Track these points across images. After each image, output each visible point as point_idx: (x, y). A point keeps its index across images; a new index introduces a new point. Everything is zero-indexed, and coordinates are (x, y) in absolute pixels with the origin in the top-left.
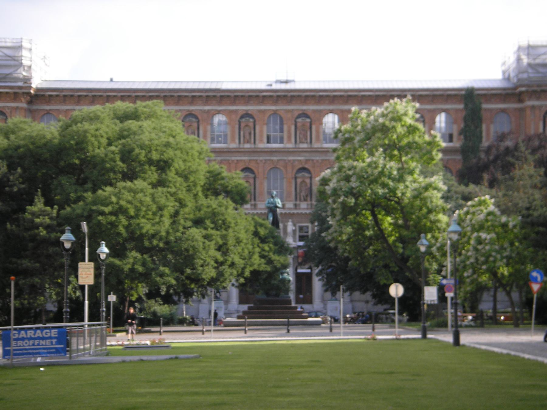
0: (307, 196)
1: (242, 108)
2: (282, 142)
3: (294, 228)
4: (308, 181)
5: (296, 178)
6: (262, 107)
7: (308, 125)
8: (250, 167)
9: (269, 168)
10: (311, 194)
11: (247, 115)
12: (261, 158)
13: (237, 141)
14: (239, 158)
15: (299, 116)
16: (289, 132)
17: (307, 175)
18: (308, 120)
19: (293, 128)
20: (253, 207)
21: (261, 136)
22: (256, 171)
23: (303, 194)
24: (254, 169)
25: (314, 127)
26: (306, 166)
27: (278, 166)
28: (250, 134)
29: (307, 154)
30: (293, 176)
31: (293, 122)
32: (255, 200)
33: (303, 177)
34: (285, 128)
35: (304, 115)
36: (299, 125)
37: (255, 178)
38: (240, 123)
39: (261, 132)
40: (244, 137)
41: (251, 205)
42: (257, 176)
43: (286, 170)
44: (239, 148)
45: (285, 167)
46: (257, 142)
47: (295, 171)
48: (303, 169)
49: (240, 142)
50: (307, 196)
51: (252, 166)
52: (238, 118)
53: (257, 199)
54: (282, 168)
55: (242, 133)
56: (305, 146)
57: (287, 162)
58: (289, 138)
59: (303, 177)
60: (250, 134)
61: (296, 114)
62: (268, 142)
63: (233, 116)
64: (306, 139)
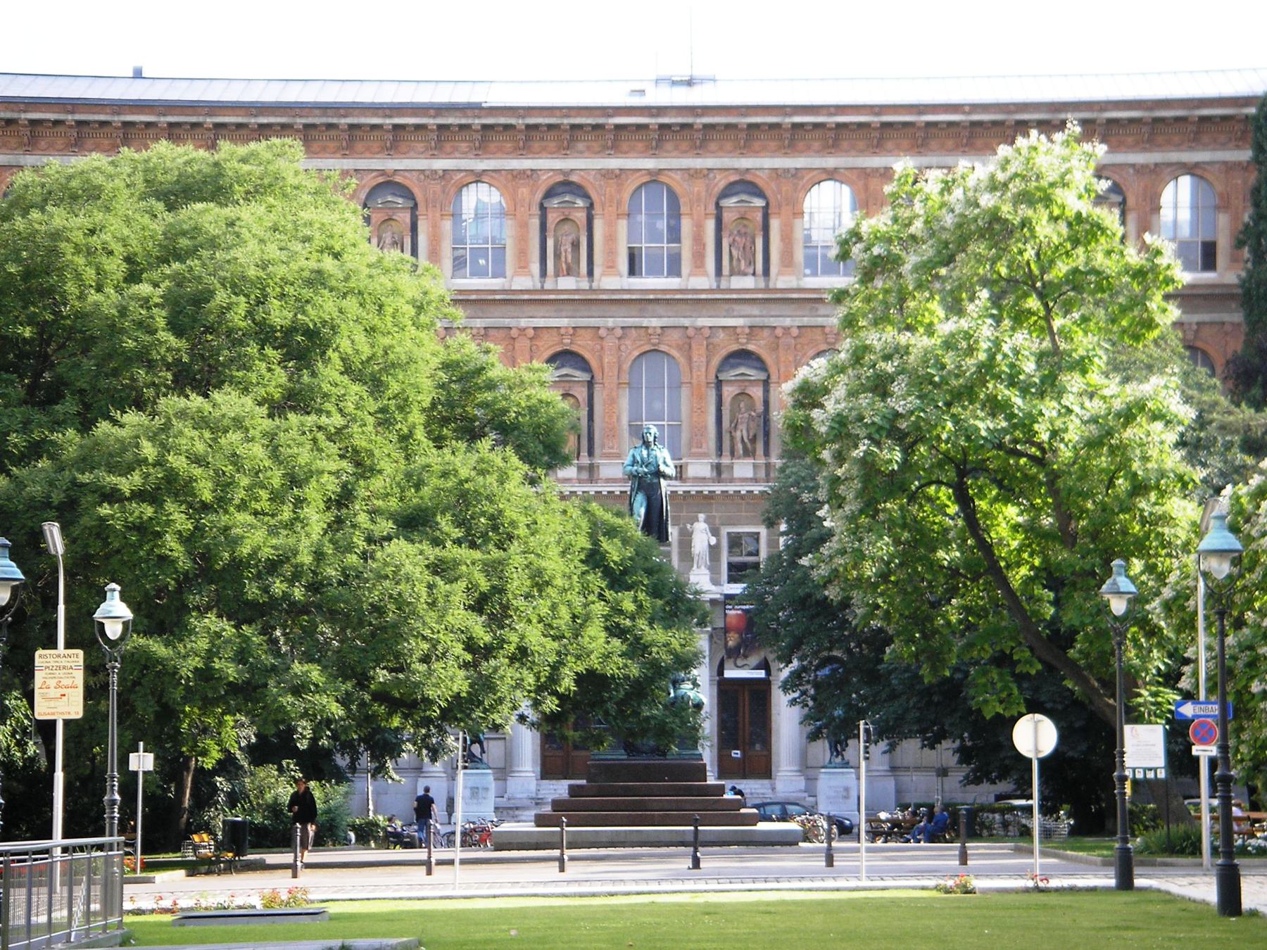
0: (753, 440)
1: (549, 164)
2: (675, 270)
3: (713, 541)
4: (757, 392)
5: (719, 384)
6: (614, 163)
7: (759, 216)
8: (574, 348)
9: (636, 353)
10: (767, 434)
11: (566, 186)
12: (610, 322)
13: (535, 267)
14: (541, 322)
15: (727, 192)
16: (698, 240)
17: (754, 374)
18: (759, 203)
19: (710, 225)
20: (585, 475)
21: (611, 253)
22: (594, 364)
24: (587, 356)
25: (775, 224)
26: (751, 347)
27: (663, 348)
28: (576, 245)
29: (755, 310)
30: (712, 378)
31: (712, 209)
32: (591, 453)
33: (743, 381)
34: (686, 225)
35: (745, 185)
36: (728, 217)
37: (590, 384)
38: (543, 208)
39: (611, 239)
40: (557, 256)
41: (580, 468)
42: (598, 377)
43: (690, 359)
44: (543, 291)
45: (687, 348)
46: (597, 271)
47: (716, 361)
48: (743, 356)
49: (544, 273)
50: (753, 440)
51: (583, 346)
52: (539, 195)
53: (597, 451)
54: (674, 352)
55: (550, 243)
56: (748, 282)
57: (691, 332)
58: (699, 257)
59: (743, 381)
60: (576, 245)
61: (721, 182)
62: (633, 271)
63: (524, 191)
64: (752, 262)
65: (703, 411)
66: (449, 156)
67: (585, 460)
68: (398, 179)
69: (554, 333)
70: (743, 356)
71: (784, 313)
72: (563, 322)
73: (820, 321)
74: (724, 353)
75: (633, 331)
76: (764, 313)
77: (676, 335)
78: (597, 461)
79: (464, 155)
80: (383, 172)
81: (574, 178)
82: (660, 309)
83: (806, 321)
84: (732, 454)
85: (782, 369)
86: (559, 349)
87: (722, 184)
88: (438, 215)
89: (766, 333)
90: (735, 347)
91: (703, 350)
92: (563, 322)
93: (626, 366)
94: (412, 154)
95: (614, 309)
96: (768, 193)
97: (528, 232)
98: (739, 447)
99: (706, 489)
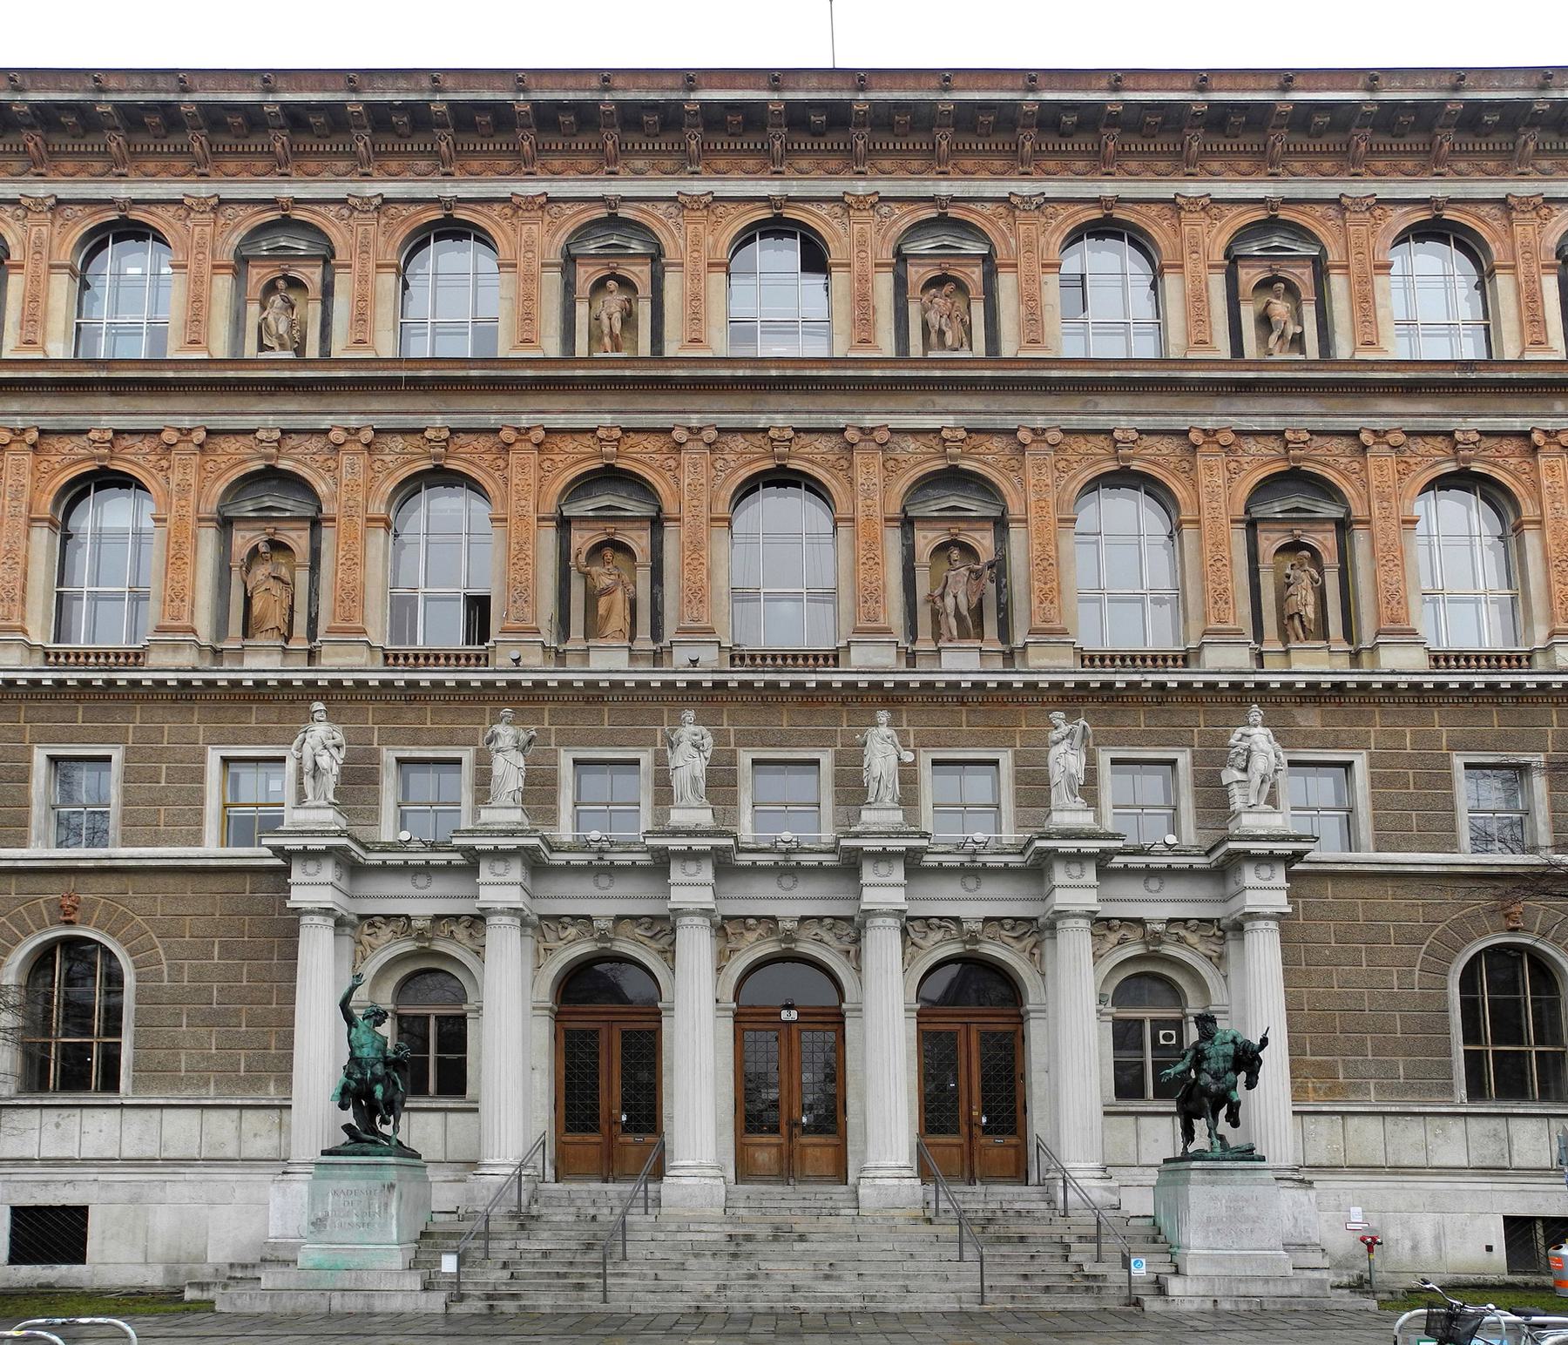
0: (978, 612)
7: (974, 275)
9: (745, 473)
10: (1005, 612)
12: (695, 420)
14: (560, 421)
17: (975, 506)
18: (974, 248)
23: (959, 595)
24: (650, 476)
25: (1006, 283)
28: (629, 318)
29: (975, 403)
33: (955, 517)
41: (633, 657)
50: (978, 612)
51: (641, 458)
52: (561, 239)
55: (582, 310)
59: (955, 517)
60: (629, 318)
61: (905, 218)
65: (875, 561)
66: (393, 176)
67: (644, 642)
68: (299, 214)
69: (587, 440)
70: (954, 478)
71: (1035, 409)
72: (607, 419)
73: (1102, 422)
74: (918, 472)
75: (739, 437)
76: (994, 408)
77: (823, 444)
78: (666, 642)
79: (422, 176)
80: (272, 203)
81: (625, 212)
82: (790, 402)
83: (1074, 422)
84: (937, 636)
85: (1032, 498)
86: (595, 464)
87: (906, 222)
88: (371, 266)
89: (997, 443)
90: (939, 465)
91: (876, 466)
92: (607, 419)
93: (727, 493)
94: (327, 175)
95: (700, 402)
96: (994, 236)
97: (539, 288)
98: (953, 622)
99: (889, 680)
